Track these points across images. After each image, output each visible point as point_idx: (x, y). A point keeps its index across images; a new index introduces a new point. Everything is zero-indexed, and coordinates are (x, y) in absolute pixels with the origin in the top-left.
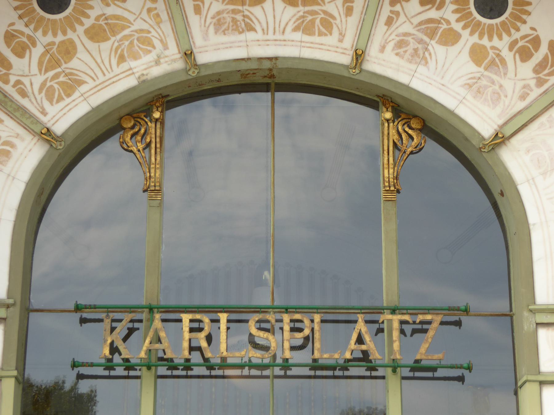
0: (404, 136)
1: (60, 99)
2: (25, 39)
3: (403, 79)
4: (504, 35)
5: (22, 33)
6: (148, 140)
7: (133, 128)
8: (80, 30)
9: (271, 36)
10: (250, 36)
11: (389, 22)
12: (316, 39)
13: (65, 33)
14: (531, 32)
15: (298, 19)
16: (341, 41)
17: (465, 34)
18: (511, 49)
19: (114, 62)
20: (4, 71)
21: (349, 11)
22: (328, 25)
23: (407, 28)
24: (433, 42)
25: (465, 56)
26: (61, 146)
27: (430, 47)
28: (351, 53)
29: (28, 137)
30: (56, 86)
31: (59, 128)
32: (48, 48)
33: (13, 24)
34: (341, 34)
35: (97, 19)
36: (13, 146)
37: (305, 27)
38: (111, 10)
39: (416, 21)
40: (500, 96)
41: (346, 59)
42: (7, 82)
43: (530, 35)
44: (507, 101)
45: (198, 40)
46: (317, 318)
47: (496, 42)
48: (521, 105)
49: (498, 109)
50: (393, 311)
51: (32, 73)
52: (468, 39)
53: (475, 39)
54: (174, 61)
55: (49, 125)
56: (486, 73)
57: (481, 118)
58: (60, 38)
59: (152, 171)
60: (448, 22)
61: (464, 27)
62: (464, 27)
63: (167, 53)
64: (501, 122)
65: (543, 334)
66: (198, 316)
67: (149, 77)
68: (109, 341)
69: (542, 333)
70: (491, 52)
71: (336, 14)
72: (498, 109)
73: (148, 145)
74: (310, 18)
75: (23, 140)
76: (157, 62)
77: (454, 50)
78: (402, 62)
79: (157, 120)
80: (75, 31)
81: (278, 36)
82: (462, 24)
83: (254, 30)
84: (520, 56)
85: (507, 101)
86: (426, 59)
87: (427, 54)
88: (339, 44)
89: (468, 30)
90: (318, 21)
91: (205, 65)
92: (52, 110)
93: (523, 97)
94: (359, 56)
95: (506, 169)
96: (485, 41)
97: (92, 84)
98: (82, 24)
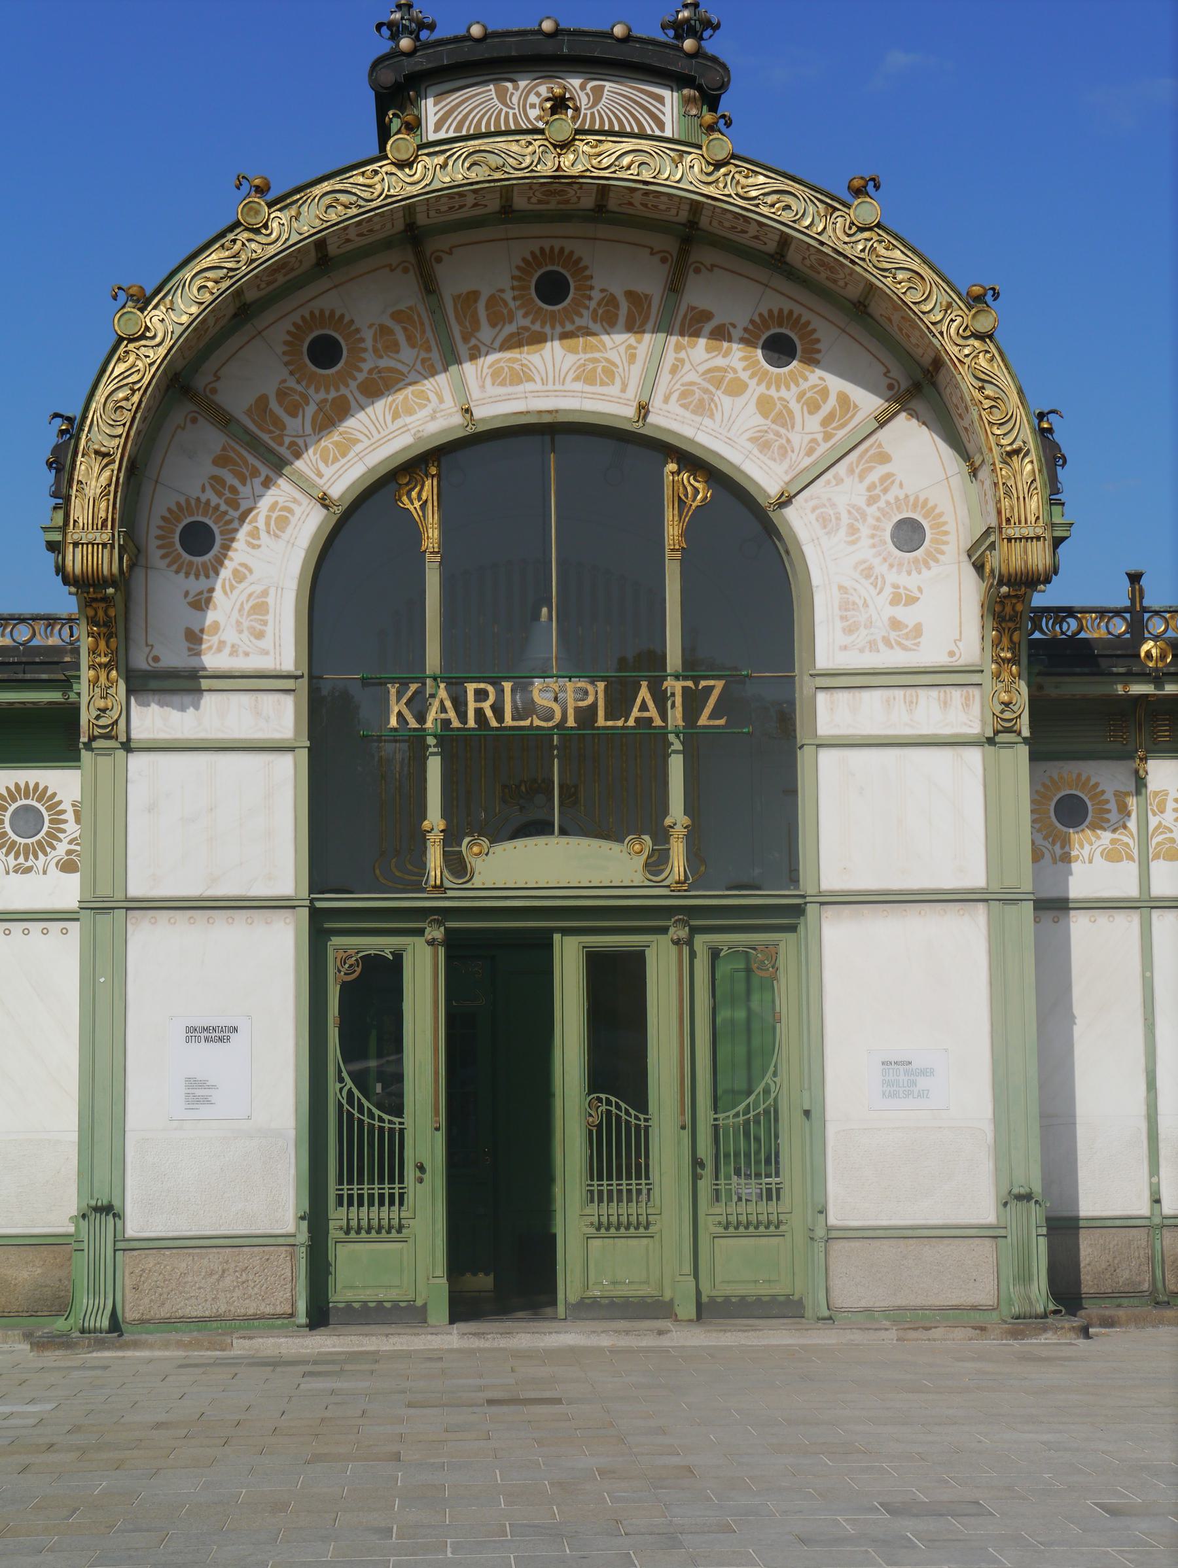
0: (689, 489)
1: (336, 460)
2: (297, 398)
3: (687, 431)
4: (792, 386)
5: (294, 391)
6: (424, 498)
7: (407, 484)
8: (353, 385)
9: (550, 387)
10: (529, 386)
11: (674, 370)
12: (598, 389)
13: (337, 389)
14: (820, 382)
15: (579, 368)
16: (623, 390)
17: (752, 383)
18: (798, 401)
19: (389, 418)
20: (278, 432)
21: (632, 358)
22: (609, 374)
23: (692, 377)
24: (719, 393)
25: (752, 407)
26: (339, 511)
27: (716, 398)
28: (635, 404)
29: (305, 500)
30: (330, 446)
31: (336, 492)
32: (321, 405)
33: (284, 381)
34: (623, 383)
35: (370, 371)
36: (290, 511)
37: (587, 376)
38: (384, 363)
39: (701, 369)
40: (786, 452)
41: (630, 412)
42: (281, 444)
43: (817, 386)
44: (794, 456)
45: (475, 392)
46: (601, 685)
47: (784, 393)
48: (807, 461)
49: (785, 465)
50: (677, 677)
51: (307, 432)
52: (755, 389)
53: (762, 389)
54: (451, 415)
55: (325, 489)
56: (774, 426)
57: (766, 476)
58: (333, 394)
59: (430, 531)
60: (735, 371)
61: (752, 377)
62: (752, 377)
63: (443, 406)
64: (787, 479)
65: (821, 697)
66: (482, 686)
67: (425, 434)
68: (396, 711)
69: (821, 697)
70: (779, 405)
71: (618, 361)
72: (785, 465)
73: (426, 501)
74: (591, 366)
75: (300, 504)
76: (433, 418)
77: (740, 401)
78: (688, 414)
79: (433, 476)
80: (347, 386)
81: (558, 387)
82: (749, 373)
83: (534, 380)
84: (808, 407)
85: (794, 456)
86: (712, 410)
87: (713, 405)
88: (622, 395)
89: (756, 380)
90: (599, 370)
91: (483, 420)
92: (327, 472)
93: (810, 452)
94: (643, 410)
95: (791, 528)
96: (773, 392)
97: (367, 442)
98: (355, 379)
